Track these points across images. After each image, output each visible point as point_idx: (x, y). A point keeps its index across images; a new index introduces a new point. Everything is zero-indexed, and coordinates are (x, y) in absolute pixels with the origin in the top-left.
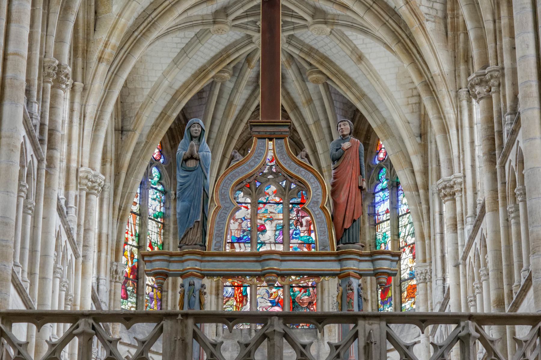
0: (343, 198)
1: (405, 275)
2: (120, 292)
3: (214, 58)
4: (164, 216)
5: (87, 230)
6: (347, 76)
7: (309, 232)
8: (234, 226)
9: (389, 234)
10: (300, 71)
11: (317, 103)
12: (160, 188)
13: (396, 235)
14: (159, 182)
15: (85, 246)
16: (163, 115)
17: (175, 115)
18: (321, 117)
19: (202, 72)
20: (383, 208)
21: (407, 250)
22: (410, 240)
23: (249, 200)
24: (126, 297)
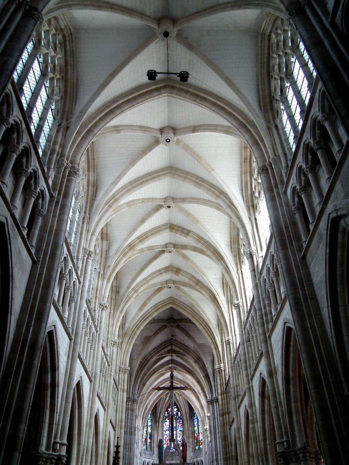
0: (184, 453)
1: (200, 439)
2: (143, 446)
3: (162, 393)
4: (151, 425)
5: (139, 439)
6: (187, 396)
7: (181, 428)
8: (165, 427)
9: (197, 429)
10: (178, 394)
11: (182, 401)
12: (150, 419)
13: (198, 430)
14: (150, 418)
15: (138, 443)
16: (152, 406)
17: (154, 406)
18: (183, 403)
19: (159, 396)
20: (196, 423)
21: (201, 433)
22: (201, 431)
23: (168, 421)
24: (144, 446)
